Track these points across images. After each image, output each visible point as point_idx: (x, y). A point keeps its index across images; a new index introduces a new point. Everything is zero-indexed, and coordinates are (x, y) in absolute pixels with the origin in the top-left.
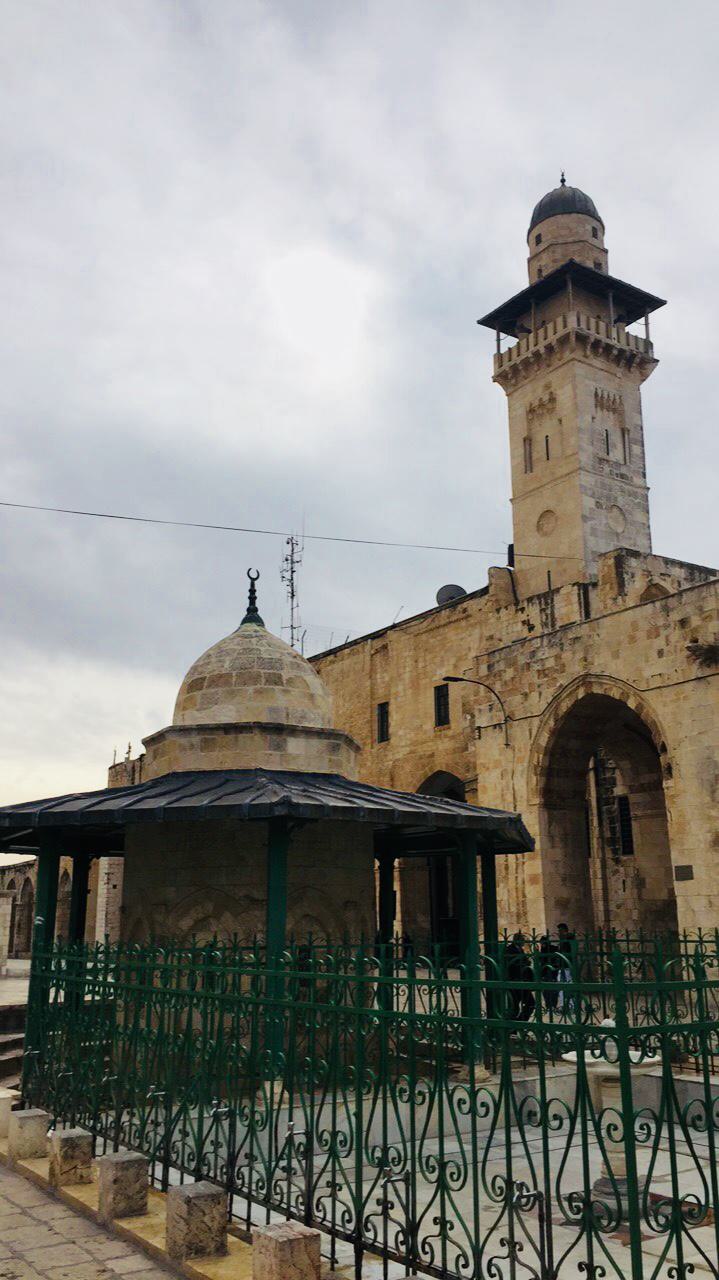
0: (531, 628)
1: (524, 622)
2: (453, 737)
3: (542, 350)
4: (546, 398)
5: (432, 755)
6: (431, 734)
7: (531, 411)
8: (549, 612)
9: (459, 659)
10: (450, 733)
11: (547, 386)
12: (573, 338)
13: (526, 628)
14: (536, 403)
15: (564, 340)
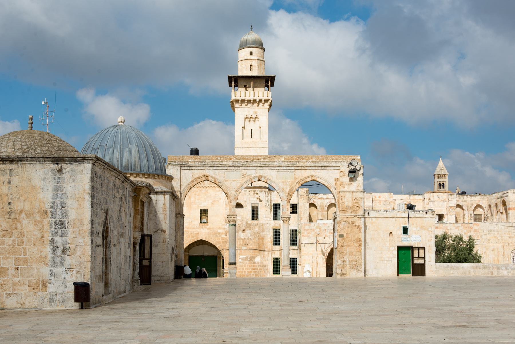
0: (261, 201)
1: (257, 198)
2: (210, 229)
3: (258, 100)
4: (254, 116)
5: (198, 234)
6: (198, 226)
7: (246, 118)
8: (269, 197)
9: (215, 201)
10: (208, 227)
11: (255, 112)
12: (269, 102)
13: (258, 201)
14: (250, 116)
15: (266, 101)
